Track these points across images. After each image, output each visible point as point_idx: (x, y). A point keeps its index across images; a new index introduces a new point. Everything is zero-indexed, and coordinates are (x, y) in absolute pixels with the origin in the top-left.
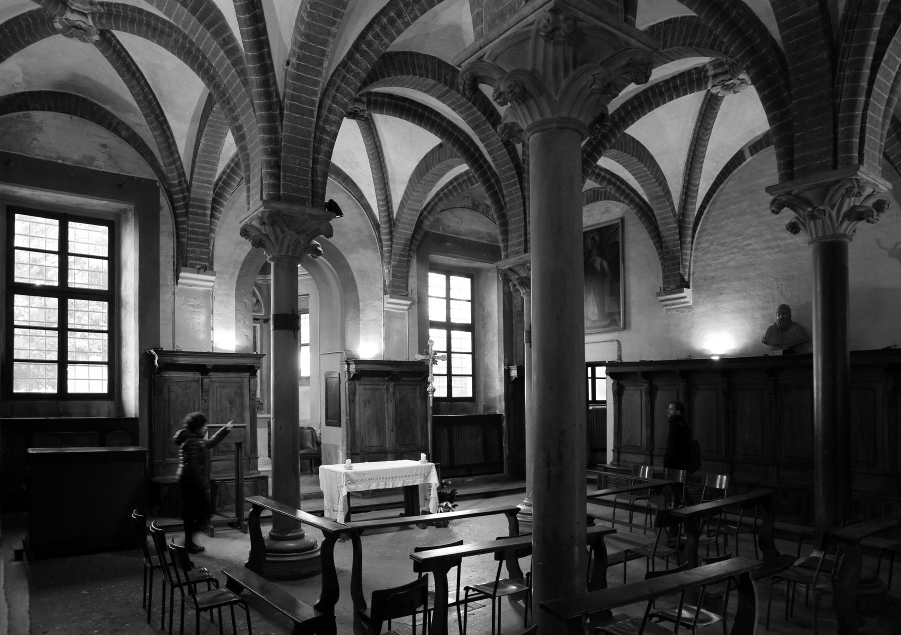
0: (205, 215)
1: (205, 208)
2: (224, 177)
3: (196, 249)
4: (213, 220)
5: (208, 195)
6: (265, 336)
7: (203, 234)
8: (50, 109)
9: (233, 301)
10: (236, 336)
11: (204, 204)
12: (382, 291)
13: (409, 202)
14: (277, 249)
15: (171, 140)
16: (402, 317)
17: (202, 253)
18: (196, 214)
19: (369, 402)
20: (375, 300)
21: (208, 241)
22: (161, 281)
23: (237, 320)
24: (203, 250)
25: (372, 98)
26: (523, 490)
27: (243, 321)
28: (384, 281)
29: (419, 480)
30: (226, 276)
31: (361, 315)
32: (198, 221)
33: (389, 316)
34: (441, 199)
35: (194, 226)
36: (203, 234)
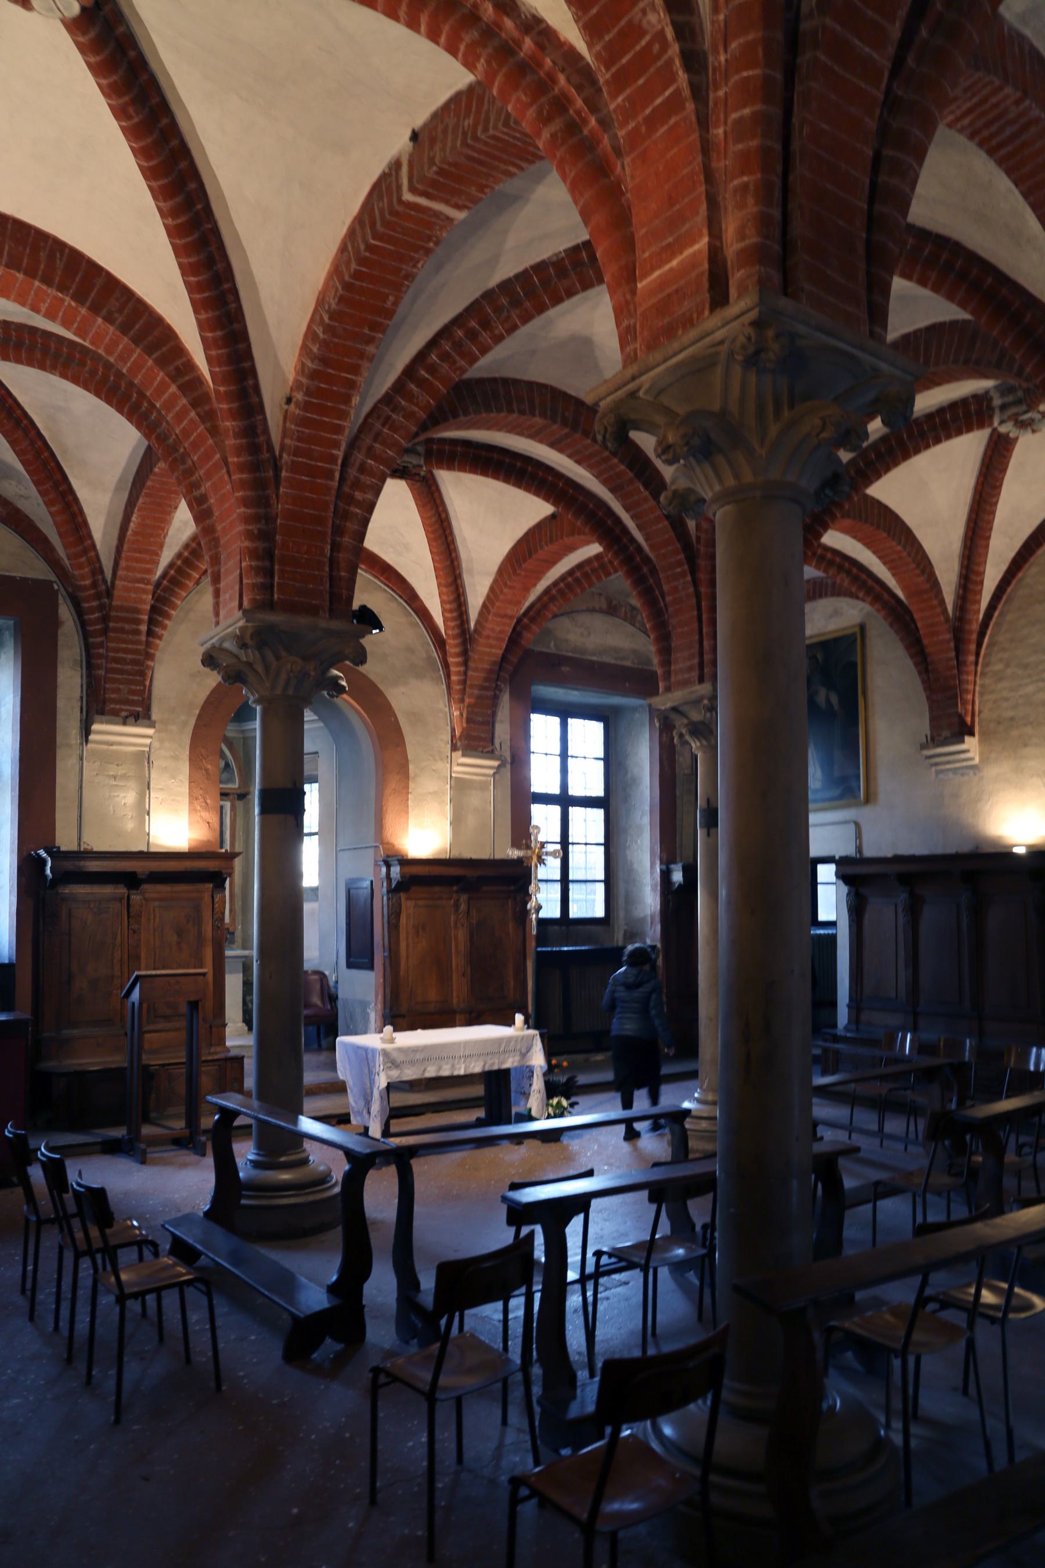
0: (137, 632)
1: (138, 622)
2: (172, 572)
3: (121, 687)
4: (151, 639)
5: (144, 602)
6: (239, 822)
7: (134, 662)
9: (185, 767)
10: (190, 823)
11: (136, 616)
12: (449, 746)
13: (497, 604)
14: (268, 685)
18: (122, 631)
21: (142, 674)
23: (192, 798)
24: (133, 687)
25: (435, 447)
26: (693, 1075)
27: (202, 800)
28: (453, 730)
30: (174, 728)
31: (411, 785)
32: (125, 642)
33: (460, 786)
34: (553, 599)
36: (134, 662)
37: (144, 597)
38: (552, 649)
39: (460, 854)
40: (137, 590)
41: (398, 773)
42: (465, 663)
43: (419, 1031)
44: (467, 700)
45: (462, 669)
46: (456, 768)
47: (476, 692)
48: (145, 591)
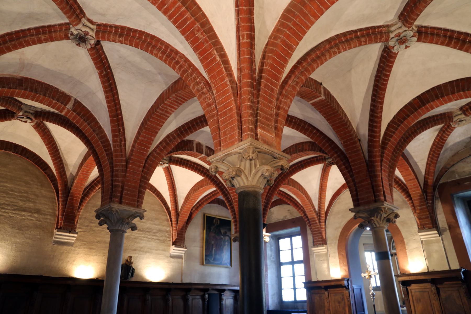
0: (316, 223)
1: (315, 221)
3: (317, 238)
4: (321, 224)
8: (274, 206)
9: (337, 255)
15: (296, 202)
16: (437, 242)
17: (319, 238)
18: (313, 224)
21: (321, 233)
23: (340, 263)
24: (319, 237)
27: (342, 263)
28: (418, 223)
30: (333, 245)
31: (407, 247)
32: (315, 226)
33: (425, 244)
35: (314, 229)
36: (318, 231)
38: (457, 177)
40: (311, 213)
41: (401, 244)
42: (411, 199)
45: (410, 202)
46: (421, 237)
47: (419, 208)
48: (313, 213)
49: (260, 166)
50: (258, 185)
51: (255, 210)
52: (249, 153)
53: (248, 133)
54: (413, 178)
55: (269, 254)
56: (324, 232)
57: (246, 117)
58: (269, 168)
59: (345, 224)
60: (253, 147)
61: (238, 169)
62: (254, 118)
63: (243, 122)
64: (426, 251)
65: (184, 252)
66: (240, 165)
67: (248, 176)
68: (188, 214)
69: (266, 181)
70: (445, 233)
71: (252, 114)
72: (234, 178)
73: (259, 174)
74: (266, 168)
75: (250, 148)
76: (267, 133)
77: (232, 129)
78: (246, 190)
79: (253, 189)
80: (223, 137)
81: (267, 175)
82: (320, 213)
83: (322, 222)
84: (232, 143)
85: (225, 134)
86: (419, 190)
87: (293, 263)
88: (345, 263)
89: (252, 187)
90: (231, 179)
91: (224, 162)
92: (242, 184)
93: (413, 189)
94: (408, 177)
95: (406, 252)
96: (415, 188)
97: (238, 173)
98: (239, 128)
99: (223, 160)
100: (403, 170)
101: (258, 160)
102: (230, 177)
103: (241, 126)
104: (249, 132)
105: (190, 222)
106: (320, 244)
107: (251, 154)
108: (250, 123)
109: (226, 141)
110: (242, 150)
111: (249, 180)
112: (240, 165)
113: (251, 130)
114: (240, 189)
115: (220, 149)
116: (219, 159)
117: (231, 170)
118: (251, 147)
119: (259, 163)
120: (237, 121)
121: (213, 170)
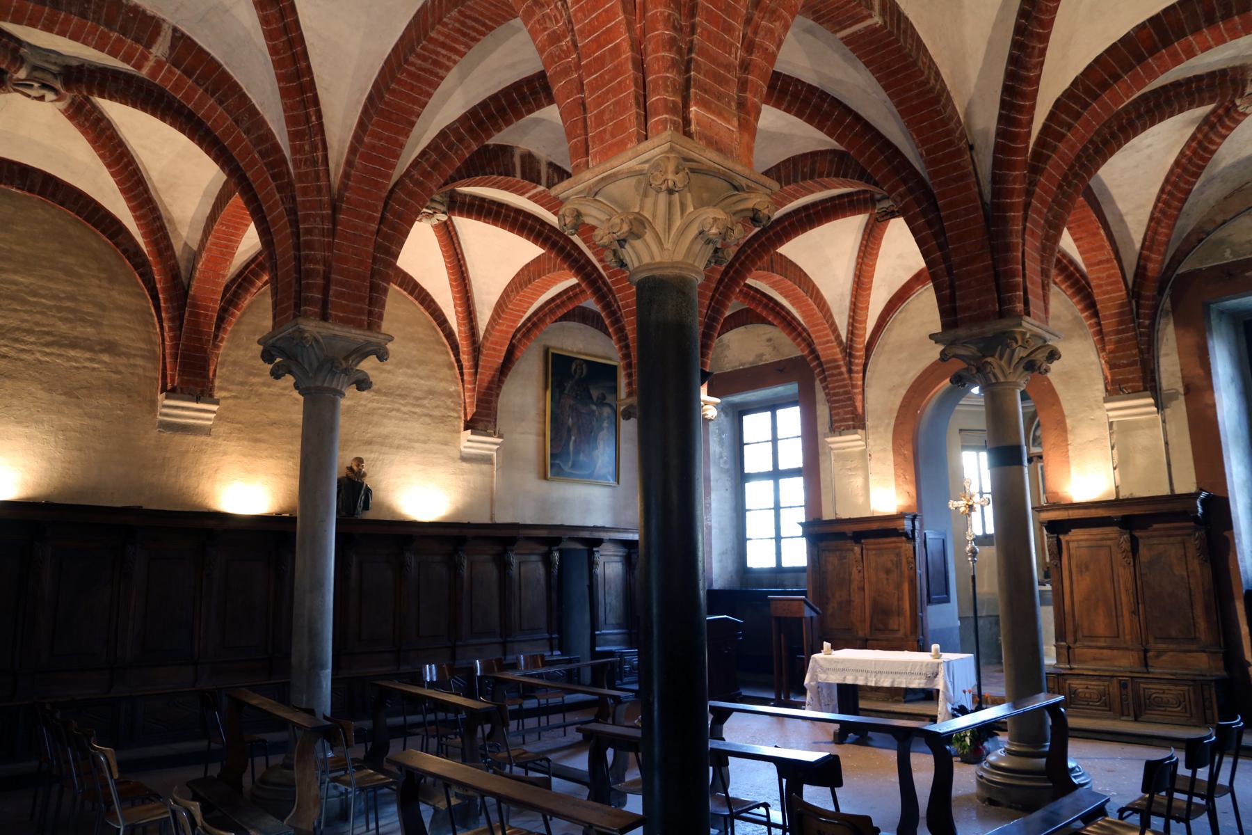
0: (841, 374)
1: (839, 367)
3: (840, 411)
9: (890, 456)
16: (1150, 425)
17: (846, 413)
18: (833, 375)
19: (1087, 568)
20: (1093, 410)
21: (852, 399)
22: (820, 451)
23: (897, 476)
28: (1106, 378)
29: (917, 681)
30: (881, 430)
31: (1070, 437)
32: (837, 381)
35: (834, 388)
36: (845, 393)
37: (835, 350)
39: (1131, 494)
41: (1056, 429)
42: (1096, 314)
43: (906, 652)
44: (1107, 347)
45: (1093, 321)
46: (1111, 414)
47: (1113, 338)
48: (833, 347)
49: (695, 208)
50: (690, 261)
51: (681, 329)
52: (666, 172)
53: (665, 116)
54: (1108, 256)
55: (715, 451)
56: (860, 397)
57: (659, 72)
58: (720, 214)
59: (915, 377)
60: (677, 155)
61: (635, 219)
62: (679, 73)
63: (650, 87)
64: (1118, 450)
65: (496, 447)
66: (642, 207)
67: (662, 236)
68: (505, 348)
69: (712, 251)
70: (1174, 403)
71: (674, 64)
72: (625, 240)
73: (693, 231)
74: (711, 213)
75: (668, 158)
76: (715, 119)
77: (620, 106)
78: (658, 273)
79: (677, 272)
80: (596, 128)
81: (714, 234)
82: (851, 347)
83: (857, 372)
84: (620, 147)
85: (600, 120)
86: (1121, 291)
87: (776, 474)
88: (910, 476)
89: (674, 265)
90: (616, 246)
91: (597, 198)
92: (646, 259)
93: (1104, 288)
94: (1094, 253)
95: (1068, 451)
96: (1110, 284)
97: (635, 230)
98: (638, 104)
99: (595, 195)
100: (1084, 235)
101: (690, 191)
102: (613, 238)
103: (645, 97)
104: (667, 114)
105: (509, 369)
106: (848, 428)
107: (670, 176)
108: (670, 89)
109: (602, 141)
110: (646, 166)
111: (665, 246)
112: (642, 207)
113: (673, 110)
114: (641, 272)
115: (587, 162)
116: (585, 189)
117: (616, 220)
118: (672, 155)
119: (693, 201)
120: (632, 84)
121: (567, 222)
